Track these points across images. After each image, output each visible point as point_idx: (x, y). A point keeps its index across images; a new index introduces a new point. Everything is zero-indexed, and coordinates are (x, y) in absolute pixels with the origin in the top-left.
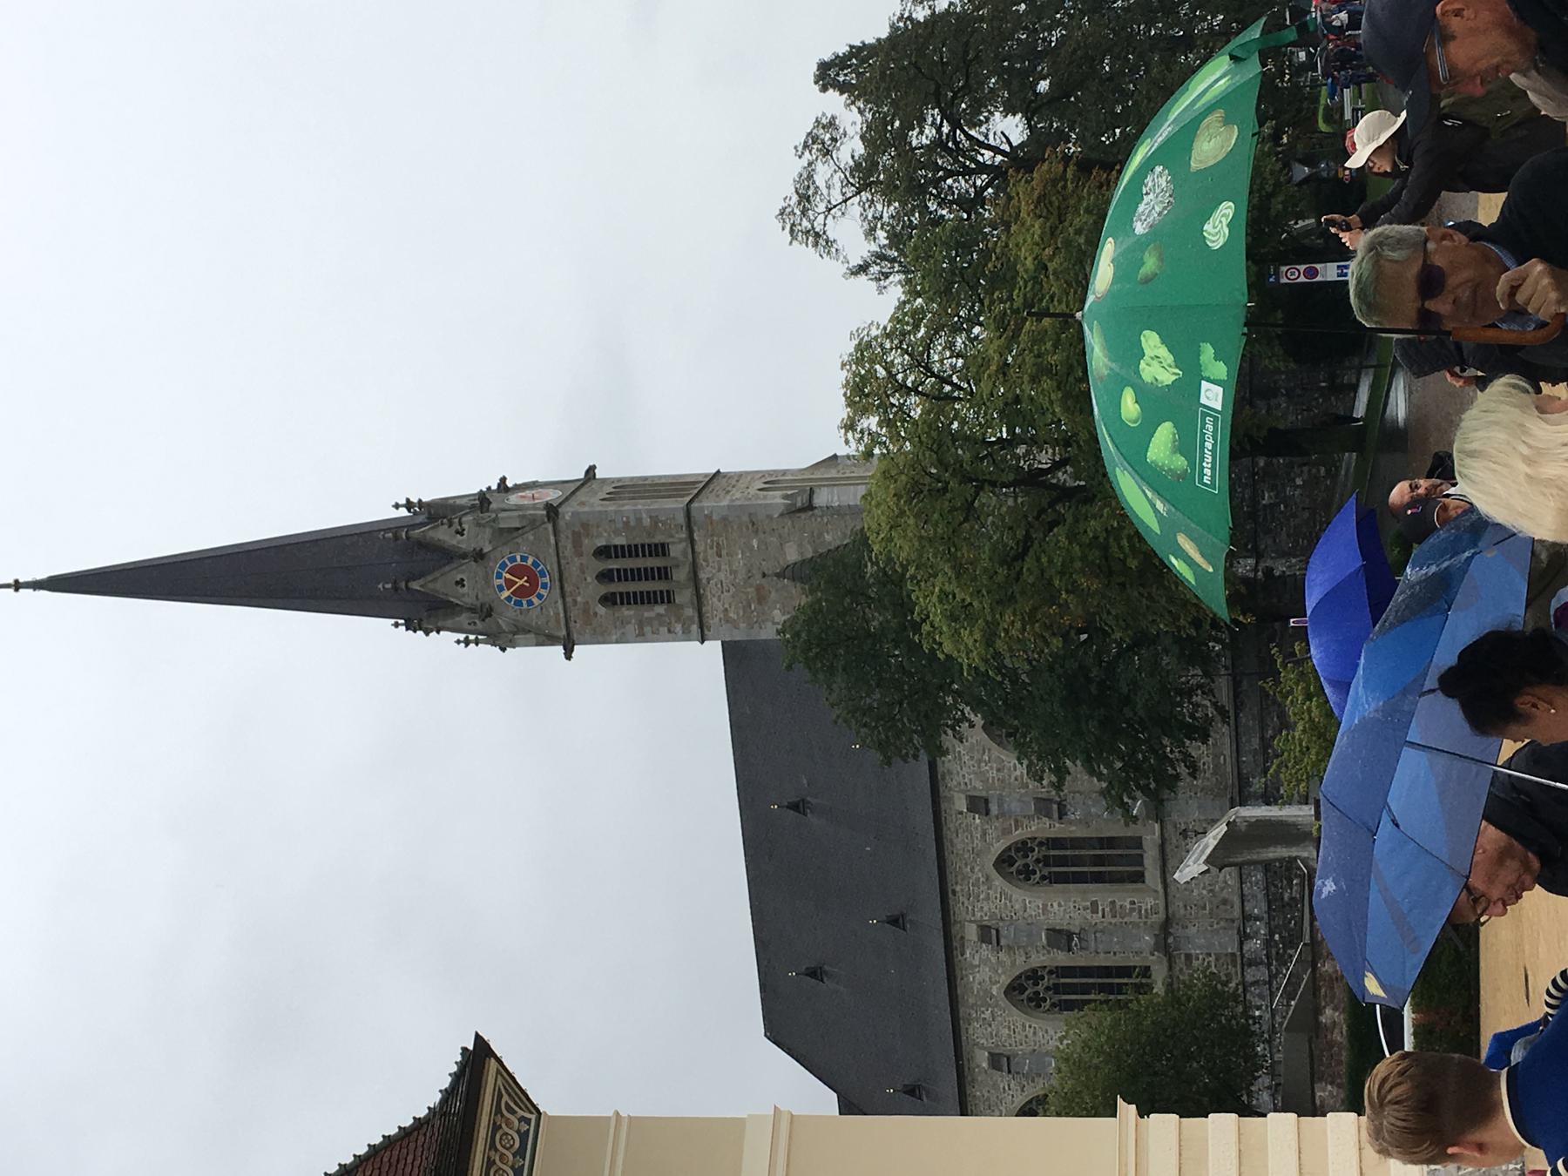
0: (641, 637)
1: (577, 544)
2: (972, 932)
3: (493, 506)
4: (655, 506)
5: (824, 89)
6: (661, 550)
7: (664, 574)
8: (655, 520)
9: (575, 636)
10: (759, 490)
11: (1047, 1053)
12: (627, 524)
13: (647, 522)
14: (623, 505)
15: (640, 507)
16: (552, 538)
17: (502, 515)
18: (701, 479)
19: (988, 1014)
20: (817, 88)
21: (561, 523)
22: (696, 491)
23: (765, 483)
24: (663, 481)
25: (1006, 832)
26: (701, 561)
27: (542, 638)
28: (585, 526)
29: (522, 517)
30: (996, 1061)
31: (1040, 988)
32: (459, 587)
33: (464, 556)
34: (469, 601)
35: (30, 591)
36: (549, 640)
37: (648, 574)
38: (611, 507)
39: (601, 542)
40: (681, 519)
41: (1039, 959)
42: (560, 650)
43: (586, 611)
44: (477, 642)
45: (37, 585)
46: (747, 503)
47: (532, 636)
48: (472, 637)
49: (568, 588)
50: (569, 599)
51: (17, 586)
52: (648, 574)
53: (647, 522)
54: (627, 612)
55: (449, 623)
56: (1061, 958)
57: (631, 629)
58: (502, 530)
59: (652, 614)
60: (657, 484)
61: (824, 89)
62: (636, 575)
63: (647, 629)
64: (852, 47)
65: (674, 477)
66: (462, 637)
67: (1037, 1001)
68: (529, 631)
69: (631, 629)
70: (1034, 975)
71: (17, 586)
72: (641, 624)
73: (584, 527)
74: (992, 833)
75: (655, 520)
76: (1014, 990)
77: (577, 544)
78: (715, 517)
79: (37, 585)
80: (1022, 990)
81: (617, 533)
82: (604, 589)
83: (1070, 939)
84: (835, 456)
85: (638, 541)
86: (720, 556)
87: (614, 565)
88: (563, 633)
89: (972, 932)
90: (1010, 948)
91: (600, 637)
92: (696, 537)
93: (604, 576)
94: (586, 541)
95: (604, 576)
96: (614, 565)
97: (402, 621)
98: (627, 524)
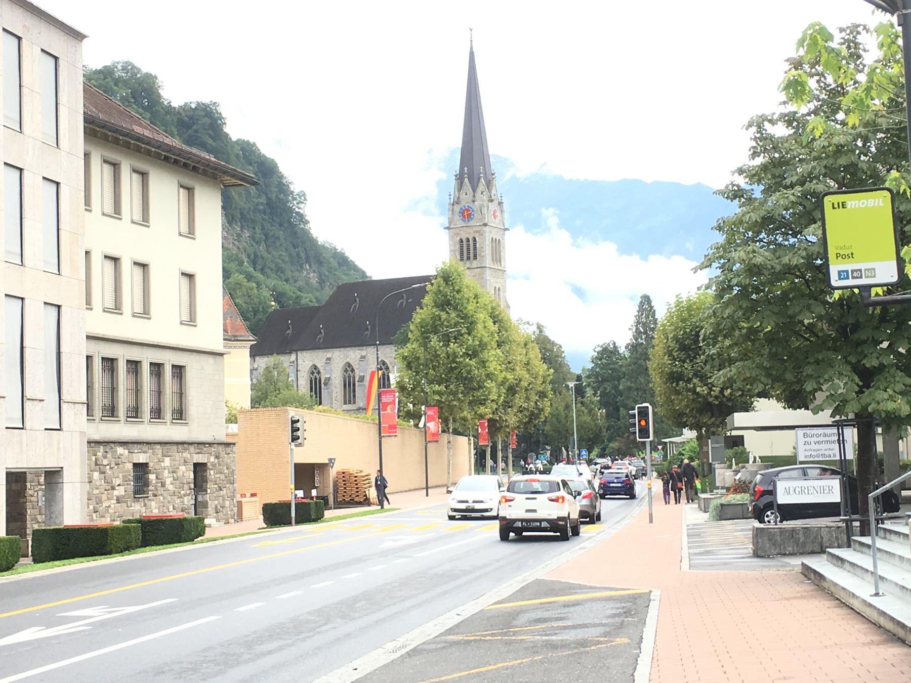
0: (451, 251)
1: (476, 232)
2: (364, 353)
3: (490, 203)
4: (487, 256)
5: (641, 297)
6: (475, 257)
7: (468, 258)
8: (483, 257)
9: (451, 230)
10: (495, 288)
11: (331, 374)
12: (482, 248)
13: (483, 254)
14: (489, 246)
15: (487, 252)
16: (478, 224)
17: (486, 208)
18: (503, 266)
19: (342, 357)
20: (641, 295)
21: (483, 227)
22: (496, 267)
23: (499, 288)
24: (502, 254)
25: (391, 363)
26: (472, 270)
27: (450, 220)
28: (482, 235)
29: (485, 214)
30: (329, 359)
31: (350, 373)
32: (464, 194)
33: (474, 194)
34: (461, 197)
35: (470, 46)
36: (450, 223)
37: (468, 253)
38: (488, 241)
39: (477, 239)
40: (483, 265)
41: (356, 371)
42: (447, 226)
43: (458, 234)
44: (450, 199)
45: (471, 48)
46: (488, 285)
47: (451, 216)
48: (452, 197)
49: (464, 228)
50: (461, 229)
51: (471, 41)
52: (468, 253)
53: (483, 254)
54: (458, 246)
55: (456, 190)
56: (357, 379)
57: (453, 248)
58: (481, 207)
59: (457, 255)
60: (500, 252)
61: (641, 297)
62: (468, 250)
63: (452, 253)
64: (653, 307)
65: (504, 257)
66: (452, 193)
67: (346, 371)
68: (452, 214)
69: (453, 248)
70: (353, 370)
71: (471, 41)
72: (454, 251)
73: (481, 234)
74: (391, 359)
75: (483, 257)
76: (349, 365)
77: (476, 232)
78: (484, 275)
79: (471, 48)
80: (349, 367)
81: (479, 245)
82: (464, 240)
83: (361, 382)
84: (509, 308)
85: (477, 249)
86: (474, 276)
87: (471, 243)
88: (451, 227)
89: (364, 353)
90: (359, 364)
91: (452, 238)
92: (479, 269)
93: (468, 240)
94: (478, 234)
95: (468, 240)
96: (471, 243)
97: (458, 173)
98: (482, 248)
